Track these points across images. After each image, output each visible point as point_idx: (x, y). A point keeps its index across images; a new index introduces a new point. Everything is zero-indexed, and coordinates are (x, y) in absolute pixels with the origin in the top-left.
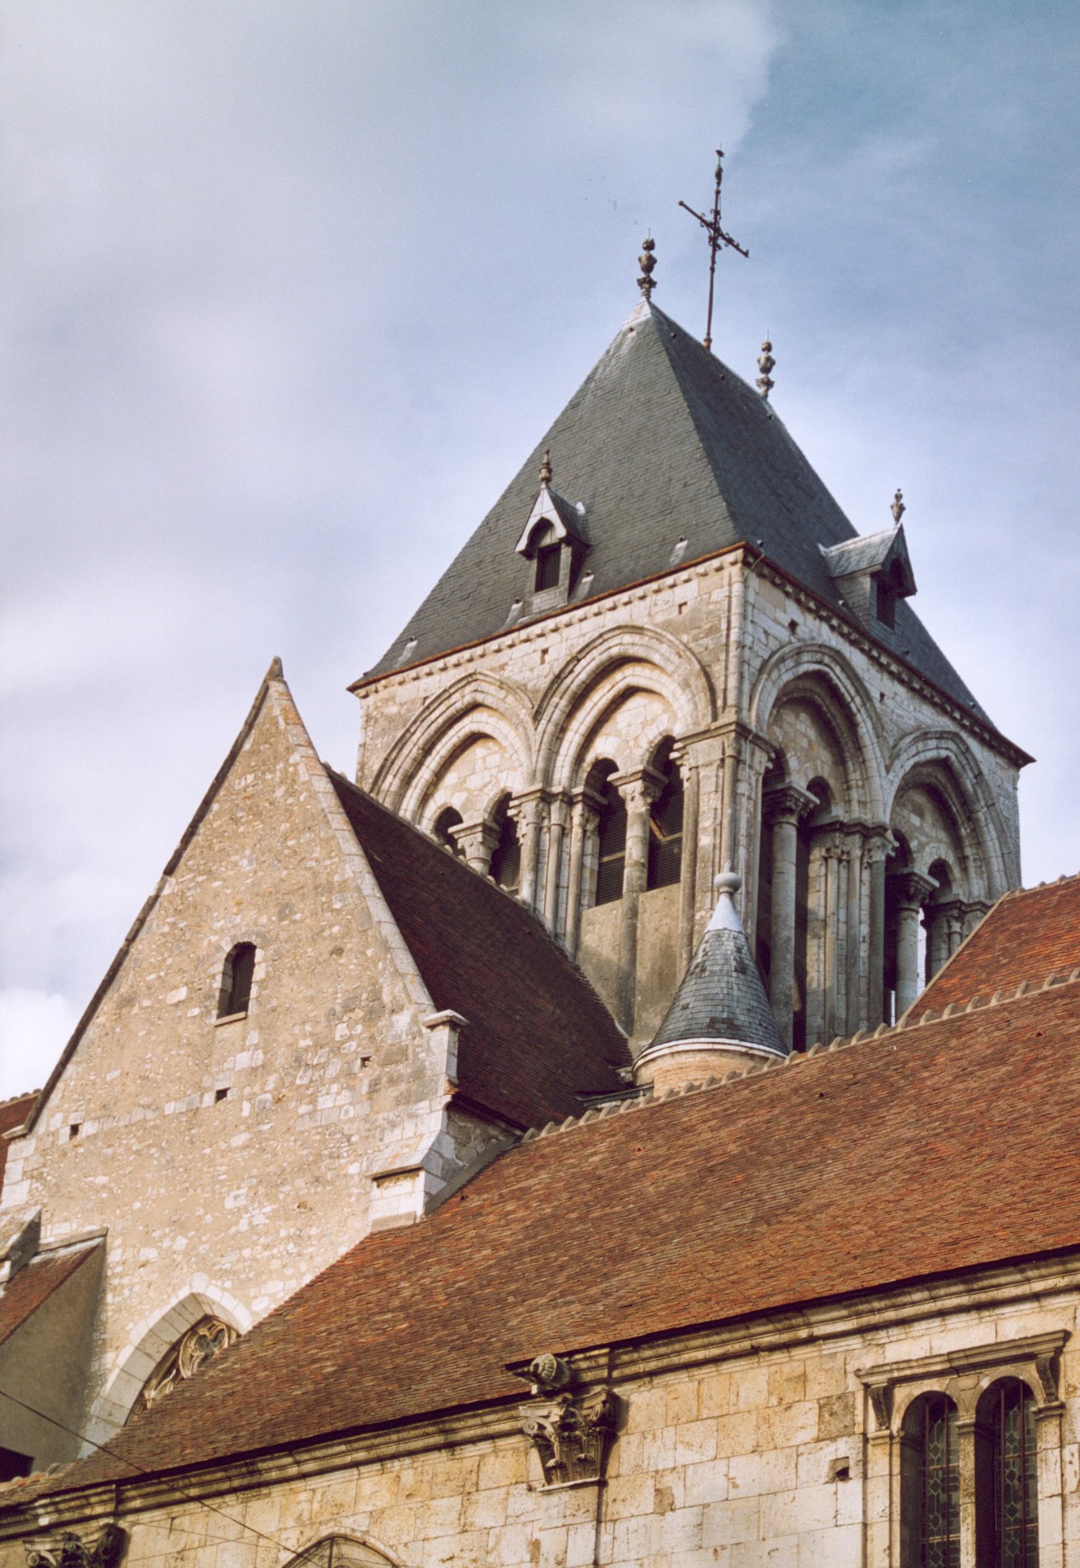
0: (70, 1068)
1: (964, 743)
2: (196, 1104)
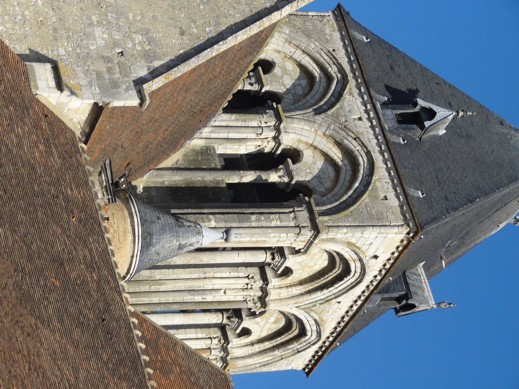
1: (314, 344)
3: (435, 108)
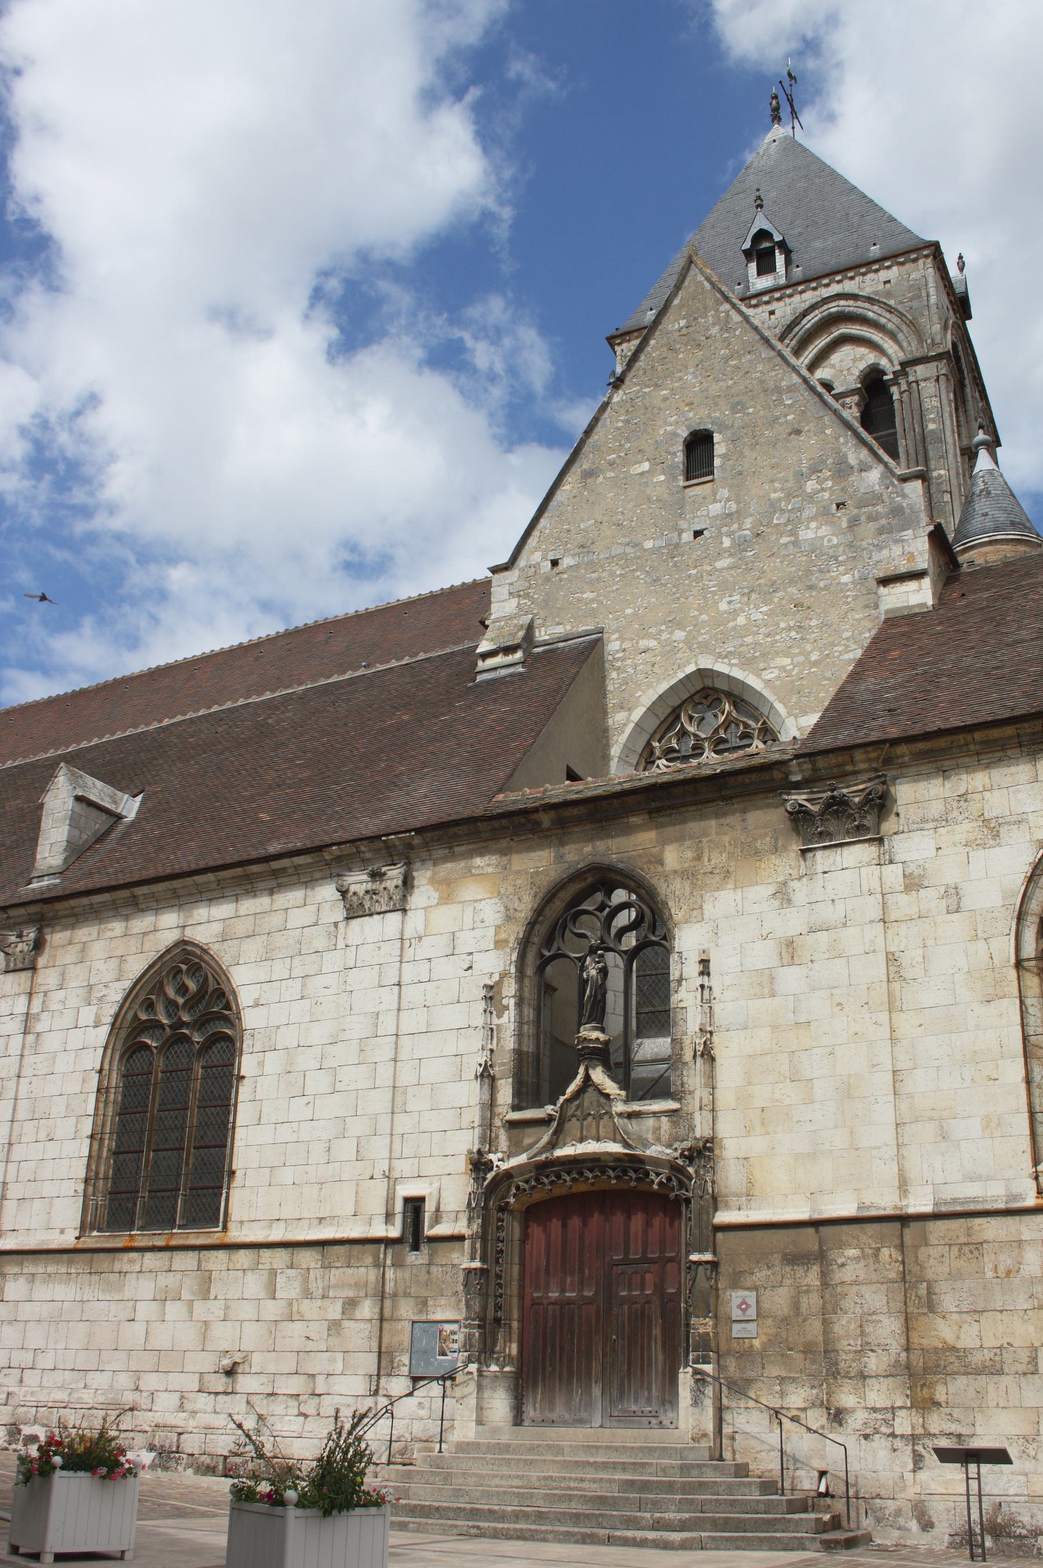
0: (543, 522)
2: (675, 540)
3: (754, 231)
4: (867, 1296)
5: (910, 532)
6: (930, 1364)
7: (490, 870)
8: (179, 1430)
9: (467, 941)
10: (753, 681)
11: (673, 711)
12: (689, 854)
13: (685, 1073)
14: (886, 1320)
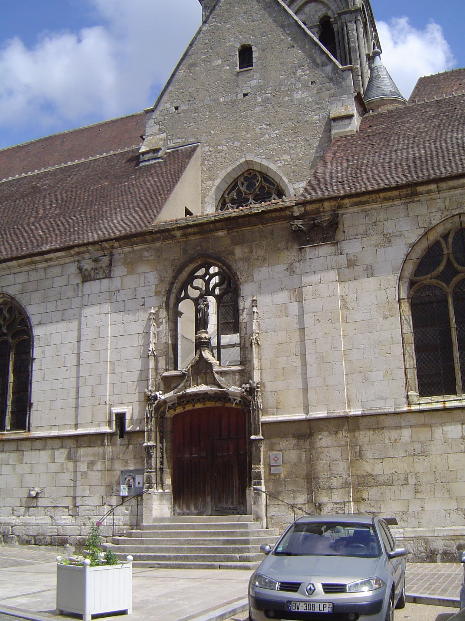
0: (170, 88)
2: (234, 98)
4: (332, 453)
5: (346, 96)
6: (360, 482)
7: (152, 258)
8: (13, 525)
9: (141, 292)
10: (273, 167)
11: (235, 180)
12: (247, 250)
13: (246, 352)
14: (340, 463)
